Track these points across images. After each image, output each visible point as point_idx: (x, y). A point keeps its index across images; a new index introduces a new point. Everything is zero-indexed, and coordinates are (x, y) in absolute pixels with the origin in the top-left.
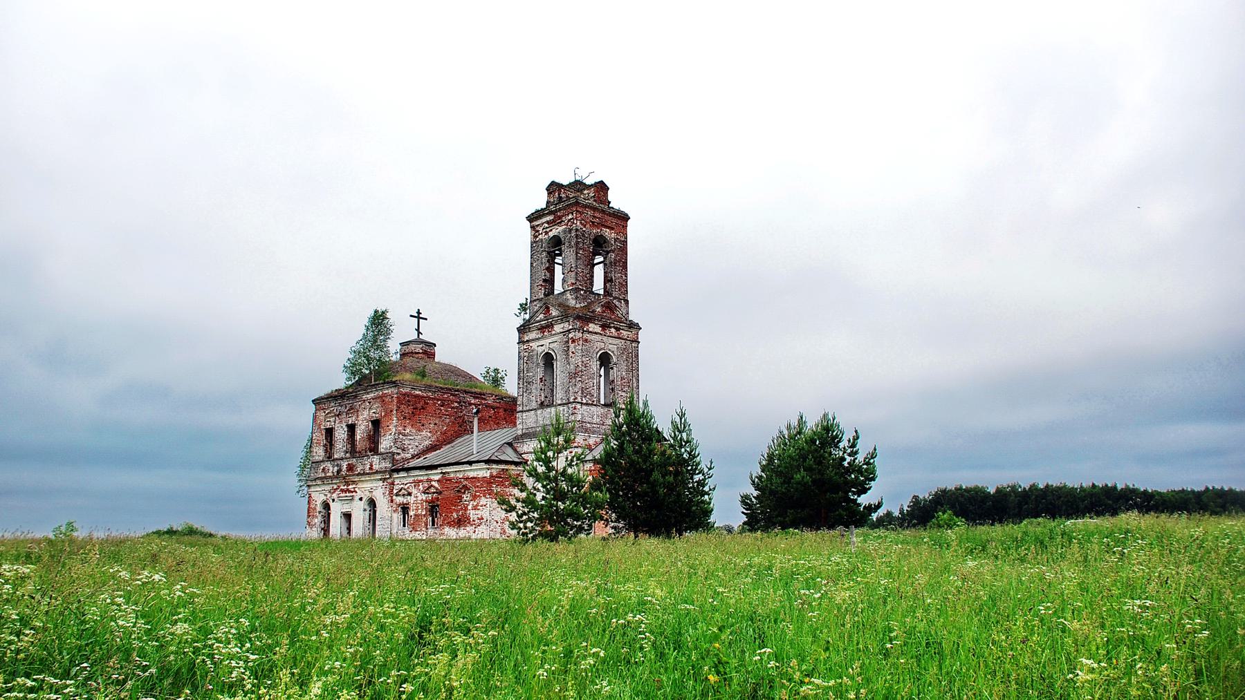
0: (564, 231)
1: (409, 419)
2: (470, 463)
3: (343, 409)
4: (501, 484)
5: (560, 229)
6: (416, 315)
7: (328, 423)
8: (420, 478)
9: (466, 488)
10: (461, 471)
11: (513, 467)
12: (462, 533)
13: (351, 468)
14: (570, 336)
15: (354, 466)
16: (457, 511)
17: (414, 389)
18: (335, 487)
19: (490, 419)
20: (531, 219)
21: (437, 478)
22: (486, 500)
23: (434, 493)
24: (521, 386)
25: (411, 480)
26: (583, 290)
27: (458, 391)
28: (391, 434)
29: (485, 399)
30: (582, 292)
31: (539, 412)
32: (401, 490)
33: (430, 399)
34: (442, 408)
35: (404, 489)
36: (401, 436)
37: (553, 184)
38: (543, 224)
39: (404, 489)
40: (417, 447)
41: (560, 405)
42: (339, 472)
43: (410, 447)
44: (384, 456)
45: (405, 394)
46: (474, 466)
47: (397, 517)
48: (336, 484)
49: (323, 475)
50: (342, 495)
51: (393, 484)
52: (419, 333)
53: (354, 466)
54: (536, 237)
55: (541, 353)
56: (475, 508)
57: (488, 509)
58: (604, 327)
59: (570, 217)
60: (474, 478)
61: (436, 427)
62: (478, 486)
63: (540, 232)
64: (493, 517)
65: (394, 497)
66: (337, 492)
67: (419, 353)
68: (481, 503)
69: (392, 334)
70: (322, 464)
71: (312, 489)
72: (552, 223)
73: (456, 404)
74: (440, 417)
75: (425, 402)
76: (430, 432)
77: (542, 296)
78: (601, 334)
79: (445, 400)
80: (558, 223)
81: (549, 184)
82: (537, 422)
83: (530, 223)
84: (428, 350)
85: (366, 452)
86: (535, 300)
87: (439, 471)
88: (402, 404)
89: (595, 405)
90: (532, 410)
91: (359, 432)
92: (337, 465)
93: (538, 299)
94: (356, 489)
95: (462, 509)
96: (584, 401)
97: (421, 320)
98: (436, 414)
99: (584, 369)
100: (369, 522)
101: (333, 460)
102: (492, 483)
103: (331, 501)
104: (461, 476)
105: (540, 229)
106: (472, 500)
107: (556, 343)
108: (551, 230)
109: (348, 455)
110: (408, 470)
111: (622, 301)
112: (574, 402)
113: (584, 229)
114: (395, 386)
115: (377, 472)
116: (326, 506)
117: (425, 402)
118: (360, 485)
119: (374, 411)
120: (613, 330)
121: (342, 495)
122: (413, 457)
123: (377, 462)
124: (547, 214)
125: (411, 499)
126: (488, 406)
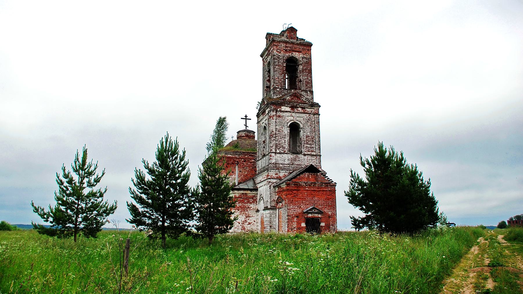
4: (242, 202)
11: (249, 192)
17: (227, 154)
26: (278, 88)
30: (278, 89)
34: (244, 163)
52: (246, 126)
58: (293, 108)
67: (244, 136)
74: (243, 168)
75: (234, 160)
78: (290, 112)
89: (286, 153)
96: (278, 151)
97: (247, 120)
99: (278, 133)
111: (309, 92)
113: (279, 54)
117: (234, 160)
120: (300, 109)
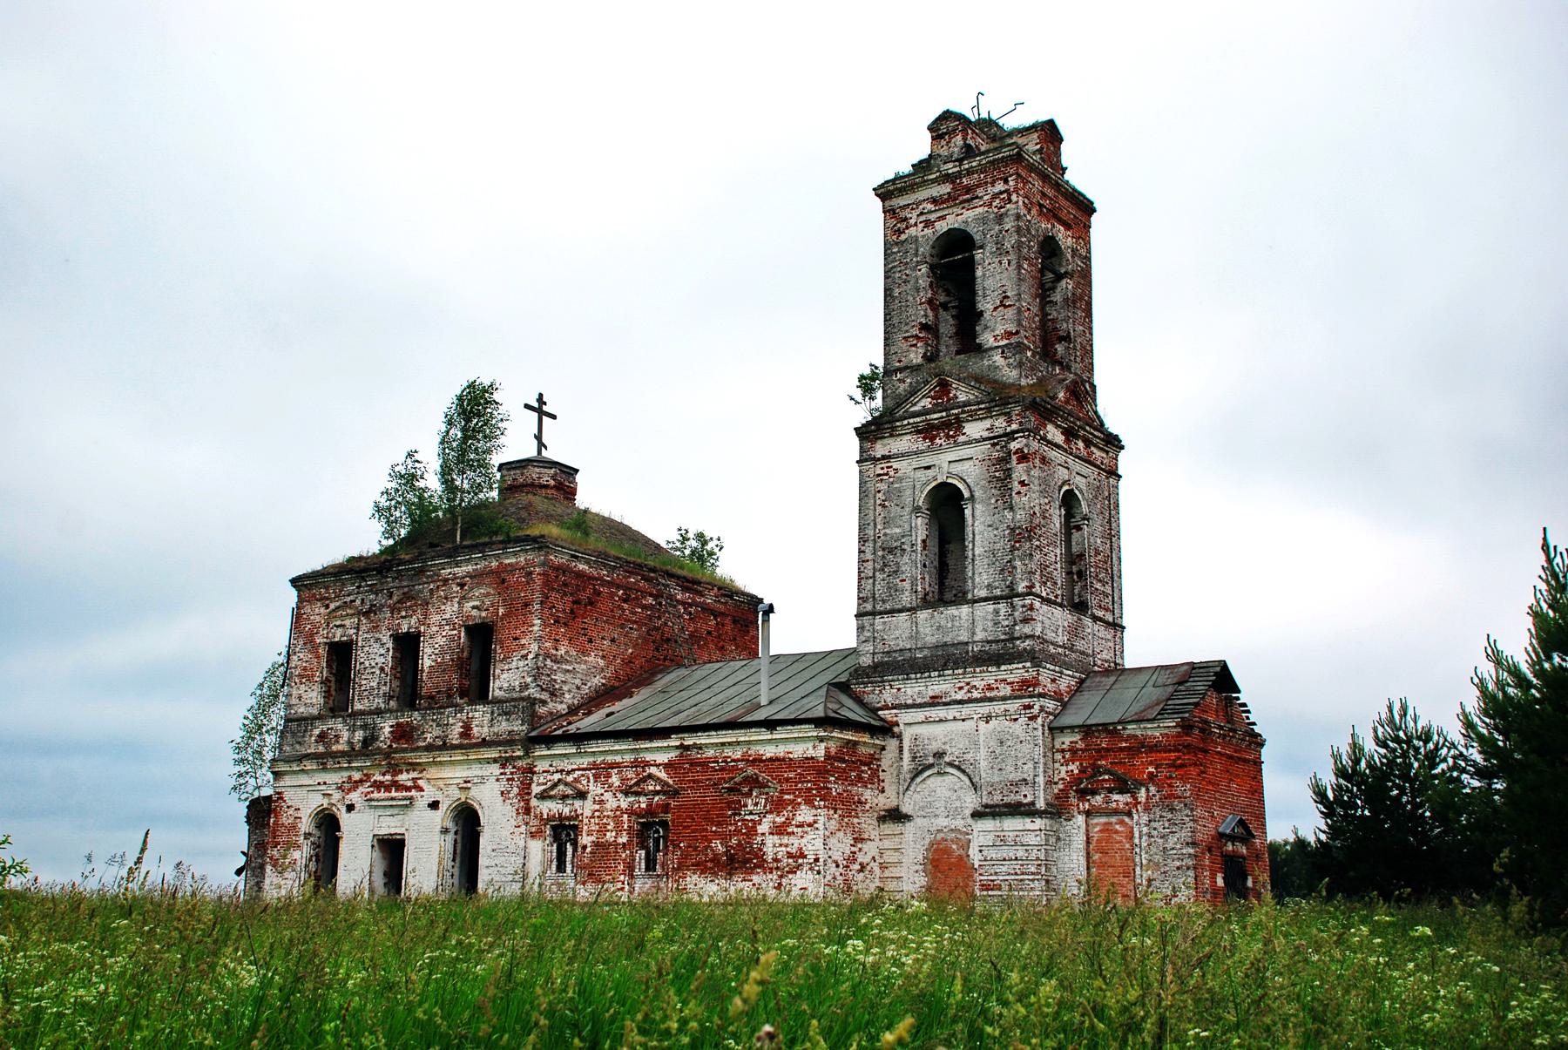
0: (983, 220)
1: (565, 624)
2: (770, 724)
3: (381, 599)
5: (969, 215)
6: (536, 405)
7: (339, 632)
8: (610, 759)
9: (754, 782)
10: (738, 743)
11: (866, 738)
12: (740, 886)
13: (403, 733)
14: (1014, 446)
15: (416, 729)
16: (725, 838)
17: (577, 557)
18: (357, 776)
19: (710, 638)
20: (886, 192)
21: (663, 758)
22: (814, 812)
23: (657, 793)
24: (869, 556)
25: (585, 761)
26: (1029, 349)
27: (653, 570)
28: (525, 657)
29: (701, 594)
31: (923, 615)
32: (555, 785)
33: (604, 583)
34: (626, 606)
35: (566, 784)
36: (548, 662)
37: (947, 116)
38: (921, 202)
39: (566, 784)
40: (578, 688)
41: (986, 599)
42: (366, 742)
43: (565, 688)
44: (505, 706)
45: (559, 569)
46: (780, 733)
47: (539, 851)
48: (358, 769)
49: (321, 749)
50: (376, 795)
51: (531, 770)
52: (541, 445)
53: (416, 729)
54: (900, 232)
55: (926, 484)
56: (779, 830)
57: (821, 832)
58: (1070, 434)
59: (1000, 187)
60: (778, 759)
61: (614, 647)
62: (787, 780)
63: (912, 222)
64: (830, 853)
65: (534, 802)
66: (361, 789)
67: (546, 487)
68: (799, 819)
69: (502, 440)
70: (317, 723)
71: (288, 781)
72: (943, 203)
73: (650, 600)
74: (622, 626)
75: (595, 589)
76: (603, 657)
77: (920, 360)
79: (630, 589)
80: (961, 202)
81: (933, 118)
82: (915, 636)
83: (883, 201)
84: (565, 479)
85: (450, 696)
86: (900, 370)
87: (674, 741)
88: (553, 589)
90: (900, 611)
91: (428, 651)
92: (364, 727)
93: (906, 368)
94: (420, 782)
95: (738, 832)
97: (545, 419)
98: (614, 617)
100: (454, 860)
101: (350, 716)
102: (828, 772)
103: (344, 809)
104: (738, 755)
105: (913, 217)
106: (771, 812)
107: (971, 462)
108: (943, 218)
109: (392, 703)
110: (580, 738)
112: (1028, 594)
113: (1029, 218)
114: (540, 549)
115: (485, 743)
116: (328, 824)
117: (595, 589)
118: (432, 772)
119: (477, 603)
120: (1081, 444)
121: (376, 795)
122: (573, 710)
123: (482, 720)
124: (933, 181)
125: (587, 808)
126: (706, 609)
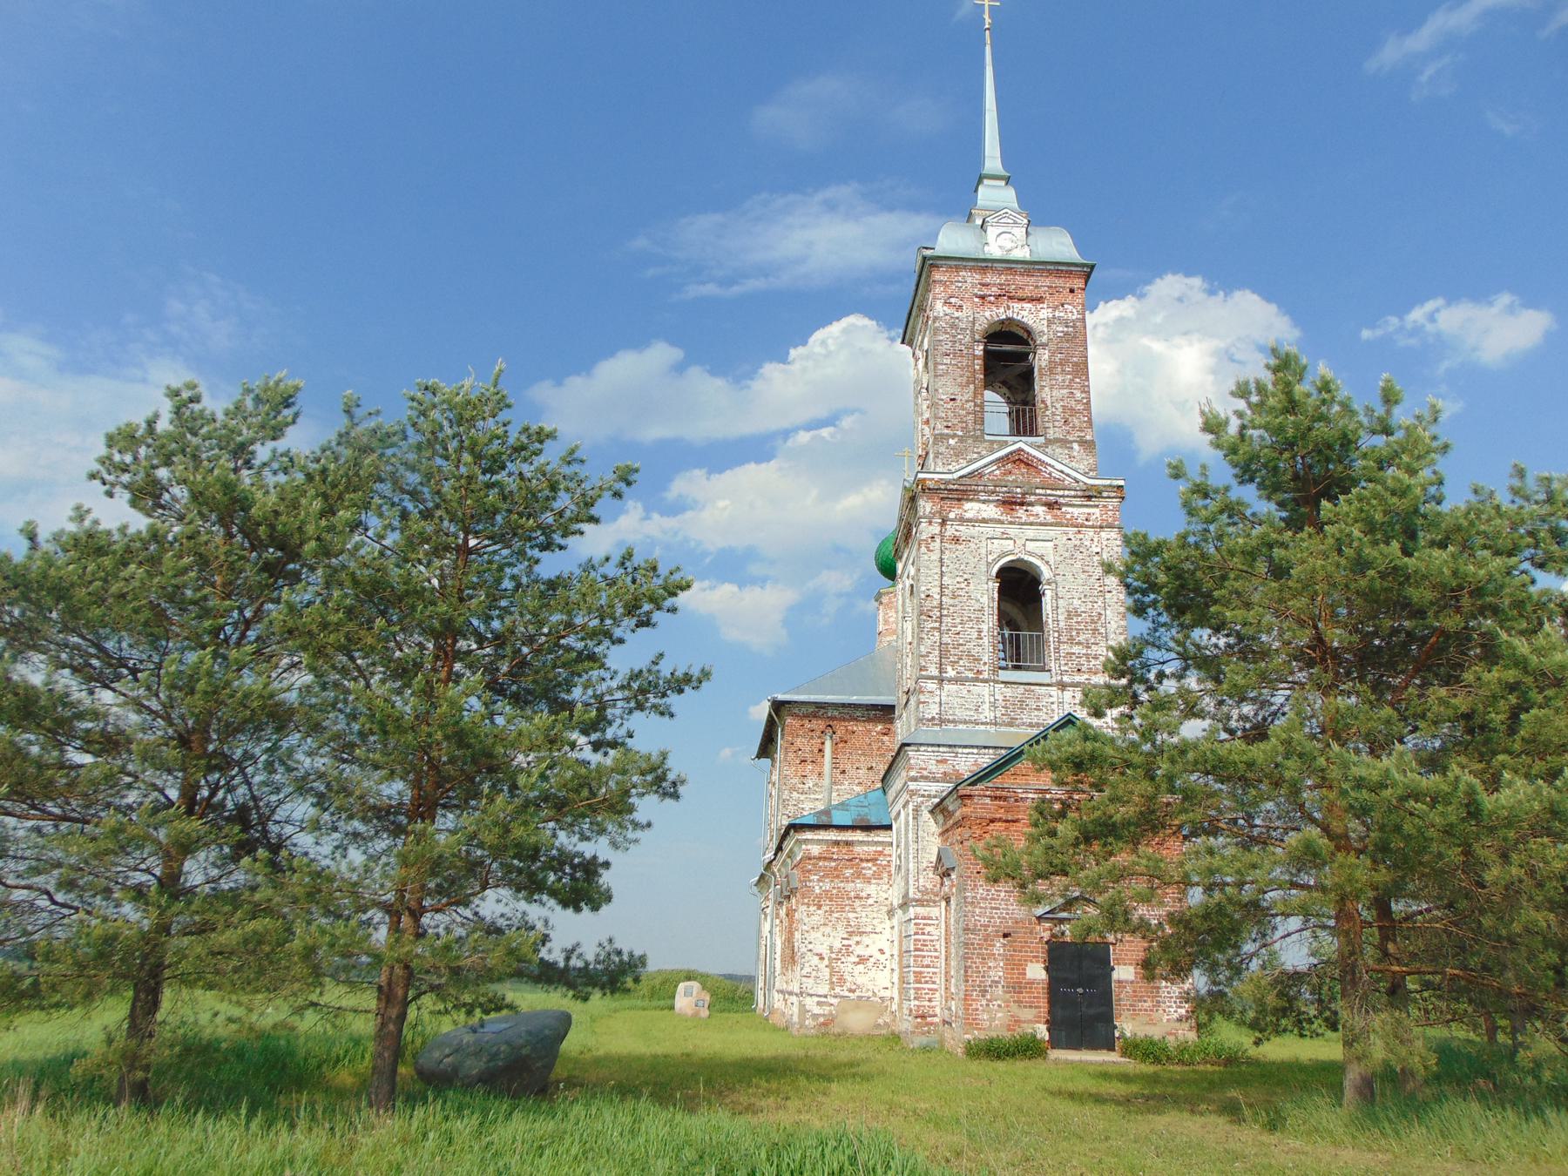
4: (835, 874)
30: (952, 442)
36: (795, 795)
64: (810, 947)
78: (1001, 522)
89: (985, 681)
96: (951, 673)
99: (952, 602)
111: (1076, 446)
113: (956, 314)
120: (1039, 509)
